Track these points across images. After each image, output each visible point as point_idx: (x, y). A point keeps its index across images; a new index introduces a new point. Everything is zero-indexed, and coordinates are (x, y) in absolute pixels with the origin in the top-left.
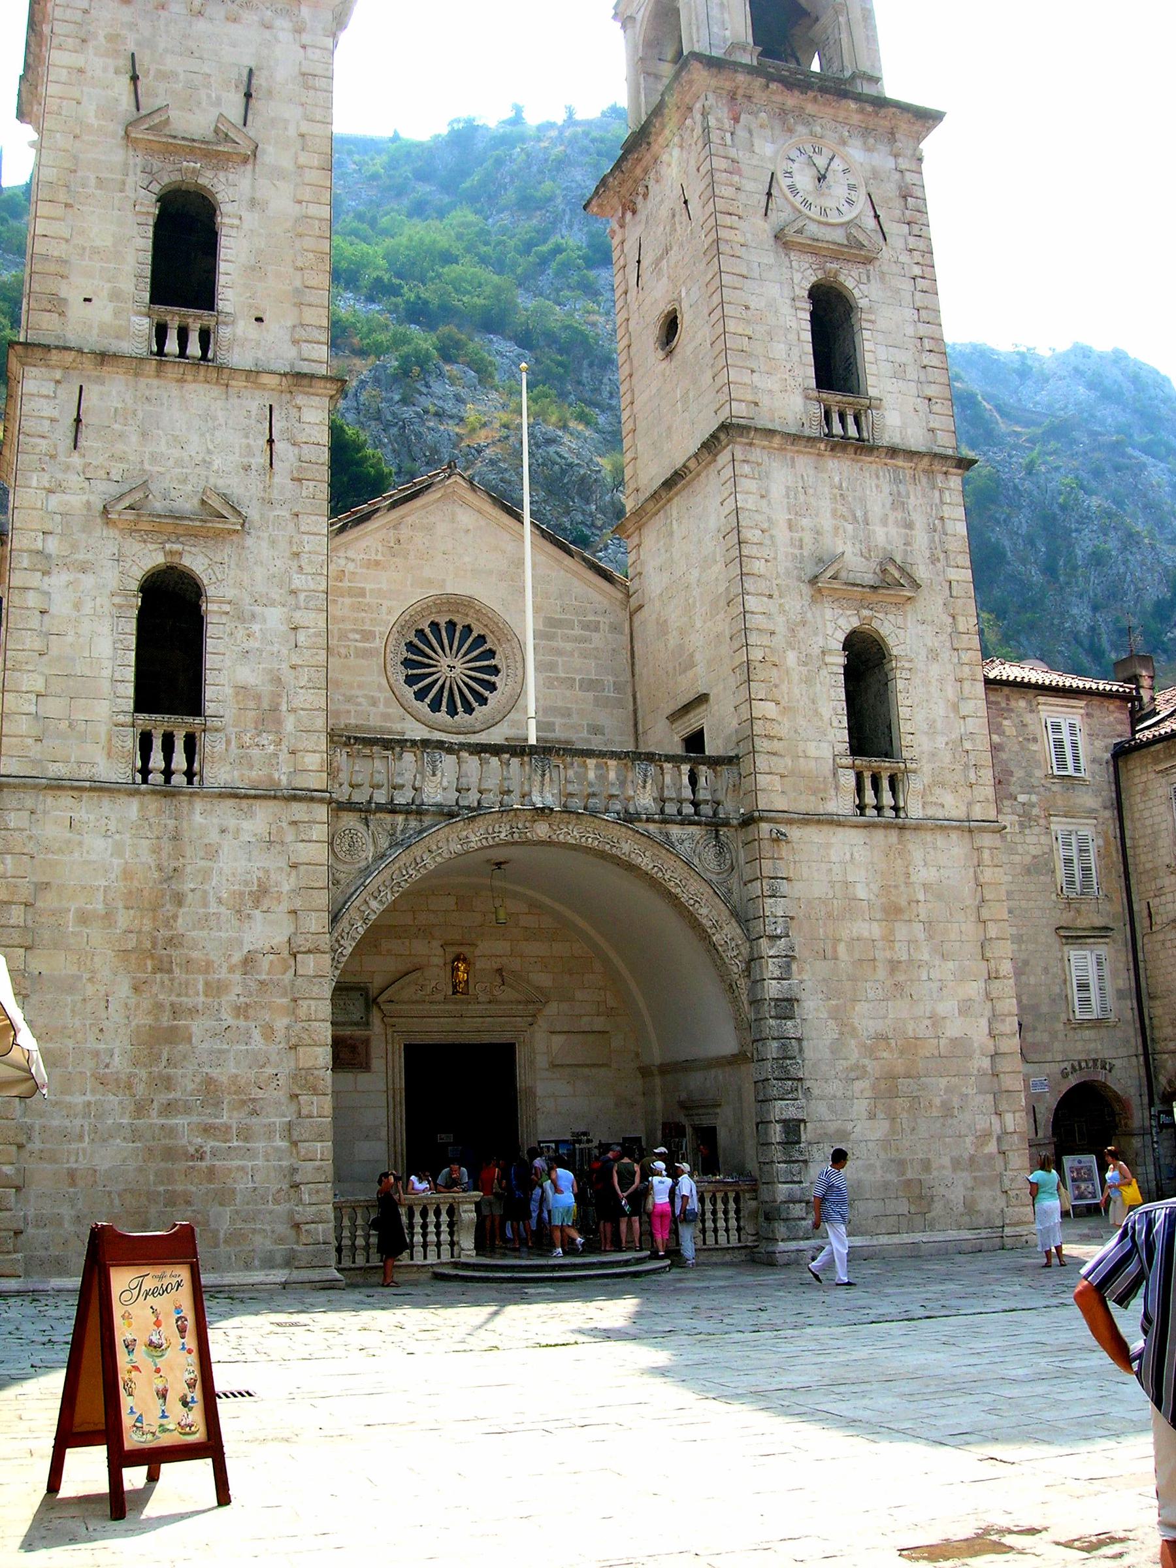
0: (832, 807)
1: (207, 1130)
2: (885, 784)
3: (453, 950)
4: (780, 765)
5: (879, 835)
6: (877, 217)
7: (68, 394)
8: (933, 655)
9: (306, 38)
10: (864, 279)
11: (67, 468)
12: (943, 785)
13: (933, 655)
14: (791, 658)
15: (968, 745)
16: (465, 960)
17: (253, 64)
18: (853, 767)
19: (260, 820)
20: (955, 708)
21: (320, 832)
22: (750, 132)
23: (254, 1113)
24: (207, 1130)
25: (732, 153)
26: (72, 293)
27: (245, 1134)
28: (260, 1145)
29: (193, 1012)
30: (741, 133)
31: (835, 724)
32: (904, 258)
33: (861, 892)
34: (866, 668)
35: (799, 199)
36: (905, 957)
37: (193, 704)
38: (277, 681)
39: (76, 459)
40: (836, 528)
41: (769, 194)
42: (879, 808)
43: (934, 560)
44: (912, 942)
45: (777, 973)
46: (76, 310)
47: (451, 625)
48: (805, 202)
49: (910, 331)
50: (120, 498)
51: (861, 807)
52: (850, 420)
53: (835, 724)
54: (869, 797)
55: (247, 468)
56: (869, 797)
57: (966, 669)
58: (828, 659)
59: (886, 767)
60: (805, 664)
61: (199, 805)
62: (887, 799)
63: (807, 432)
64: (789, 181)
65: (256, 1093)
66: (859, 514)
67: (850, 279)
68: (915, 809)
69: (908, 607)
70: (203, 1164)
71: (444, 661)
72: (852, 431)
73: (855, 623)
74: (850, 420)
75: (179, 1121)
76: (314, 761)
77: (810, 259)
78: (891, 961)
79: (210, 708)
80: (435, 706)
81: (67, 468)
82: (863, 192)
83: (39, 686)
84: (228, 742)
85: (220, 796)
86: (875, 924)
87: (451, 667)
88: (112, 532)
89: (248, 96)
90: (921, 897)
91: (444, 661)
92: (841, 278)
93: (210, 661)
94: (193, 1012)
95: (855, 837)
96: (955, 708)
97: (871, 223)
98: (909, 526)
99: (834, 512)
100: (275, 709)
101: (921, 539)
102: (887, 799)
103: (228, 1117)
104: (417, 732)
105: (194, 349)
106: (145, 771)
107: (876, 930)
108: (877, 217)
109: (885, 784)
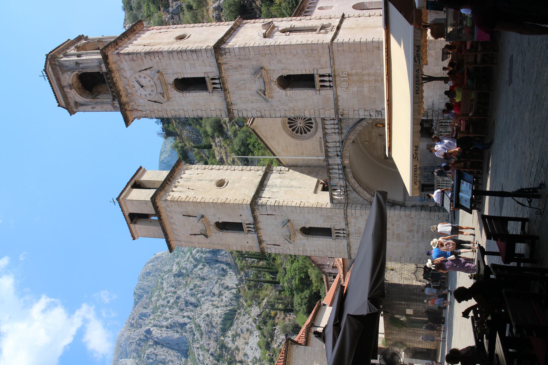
0: (331, 96)
1: (418, 232)
2: (322, 78)
3: (374, 127)
4: (322, 111)
5: (337, 83)
6: (146, 70)
7: (269, 246)
8: (280, 61)
9: (170, 206)
10: (168, 75)
11: (284, 247)
12: (320, 61)
13: (280, 61)
14: (291, 105)
15: (306, 52)
16: (376, 125)
17: (181, 216)
18: (319, 90)
19: (351, 220)
20: (294, 55)
21: (353, 211)
22: (139, 106)
23: (415, 224)
24: (418, 232)
25: (148, 112)
26: (247, 245)
27: (419, 226)
28: (421, 224)
29: (393, 233)
30: (140, 108)
31: (307, 94)
32: (155, 61)
33: (355, 89)
34: (289, 81)
35: (152, 93)
36: (373, 78)
37: (330, 229)
38: (321, 216)
39: (282, 245)
40: (249, 89)
41: (155, 102)
42: (330, 81)
43: (249, 59)
44: (369, 75)
45: (380, 116)
46: (250, 244)
47: (289, 123)
48: (152, 91)
49: (178, 61)
50: (289, 242)
51: (330, 86)
52: (214, 81)
53: (307, 94)
54: (327, 84)
55: (275, 219)
56: (327, 84)
57: (282, 51)
58: (289, 95)
59: (317, 79)
60: (292, 101)
61: (350, 229)
62: (326, 79)
63: (223, 95)
64: (148, 96)
65: (410, 224)
66: (242, 82)
67: (171, 80)
68: (328, 71)
69: (267, 69)
70: (425, 233)
71: (299, 125)
72: (217, 81)
73: (276, 86)
74: (214, 81)
75: (416, 235)
76: (338, 211)
77: (169, 92)
78: (375, 82)
79: (329, 227)
80: (311, 127)
81: (284, 247)
82: (139, 74)
83: (330, 252)
84: (336, 225)
85: (348, 227)
86: (365, 86)
87: (300, 124)
88: (296, 240)
89: (189, 216)
90: (355, 71)
91: (299, 125)
92: (171, 83)
93: (319, 226)
94: (393, 233)
95: (339, 89)
96: (294, 55)
97: (148, 71)
98: (241, 66)
99: (244, 90)
100: (327, 216)
101: (244, 63)
102: (326, 79)
103: (415, 228)
104: (320, 134)
105: (252, 226)
106: (344, 237)
107: (366, 85)
108: (146, 70)
109: (322, 78)
